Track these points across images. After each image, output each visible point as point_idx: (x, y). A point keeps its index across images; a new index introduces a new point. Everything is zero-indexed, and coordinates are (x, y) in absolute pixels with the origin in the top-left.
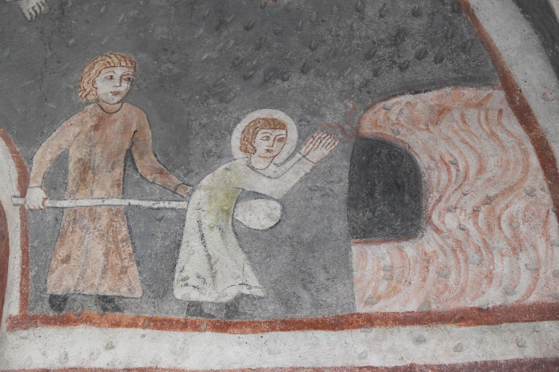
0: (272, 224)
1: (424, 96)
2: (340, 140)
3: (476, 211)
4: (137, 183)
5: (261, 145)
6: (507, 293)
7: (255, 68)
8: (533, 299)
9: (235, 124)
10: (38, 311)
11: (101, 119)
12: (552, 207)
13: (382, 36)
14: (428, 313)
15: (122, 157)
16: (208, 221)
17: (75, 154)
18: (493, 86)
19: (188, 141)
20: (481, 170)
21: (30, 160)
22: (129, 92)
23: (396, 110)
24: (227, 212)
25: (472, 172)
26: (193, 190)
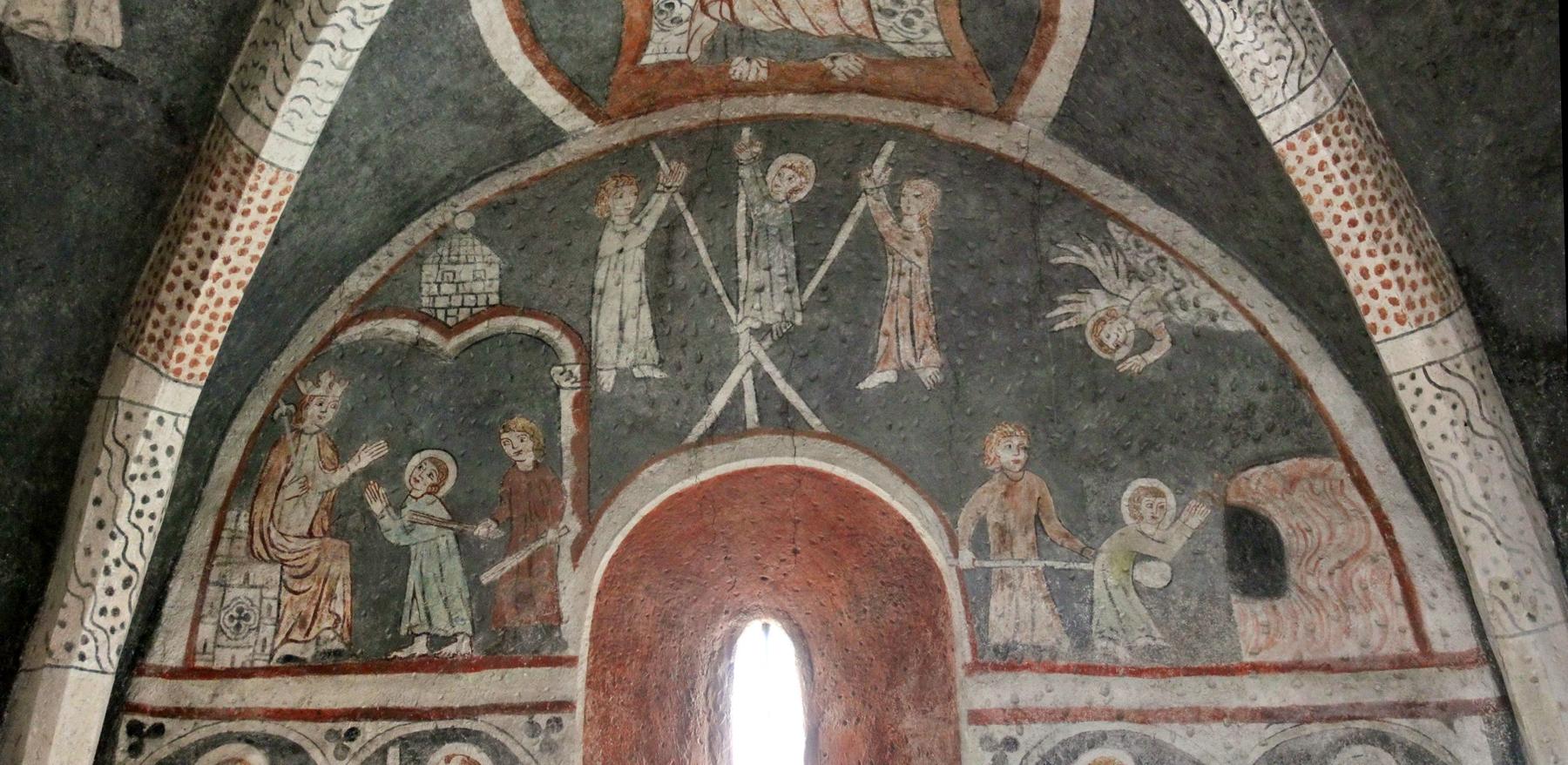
0: (1165, 583)
1: (1275, 465)
2: (1212, 508)
3: (1331, 574)
4: (1048, 546)
5: (1147, 513)
6: (1364, 645)
7: (1131, 439)
8: (1384, 651)
9: (1122, 492)
10: (986, 658)
11: (1009, 487)
12: (1393, 571)
13: (1236, 410)
14: (1301, 662)
15: (1032, 522)
16: (1111, 581)
17: (992, 518)
18: (1334, 458)
19: (1084, 507)
20: (1332, 536)
21: (955, 523)
22: (1027, 461)
23: (1254, 480)
24: (1127, 571)
25: (1324, 539)
26: (1097, 553)
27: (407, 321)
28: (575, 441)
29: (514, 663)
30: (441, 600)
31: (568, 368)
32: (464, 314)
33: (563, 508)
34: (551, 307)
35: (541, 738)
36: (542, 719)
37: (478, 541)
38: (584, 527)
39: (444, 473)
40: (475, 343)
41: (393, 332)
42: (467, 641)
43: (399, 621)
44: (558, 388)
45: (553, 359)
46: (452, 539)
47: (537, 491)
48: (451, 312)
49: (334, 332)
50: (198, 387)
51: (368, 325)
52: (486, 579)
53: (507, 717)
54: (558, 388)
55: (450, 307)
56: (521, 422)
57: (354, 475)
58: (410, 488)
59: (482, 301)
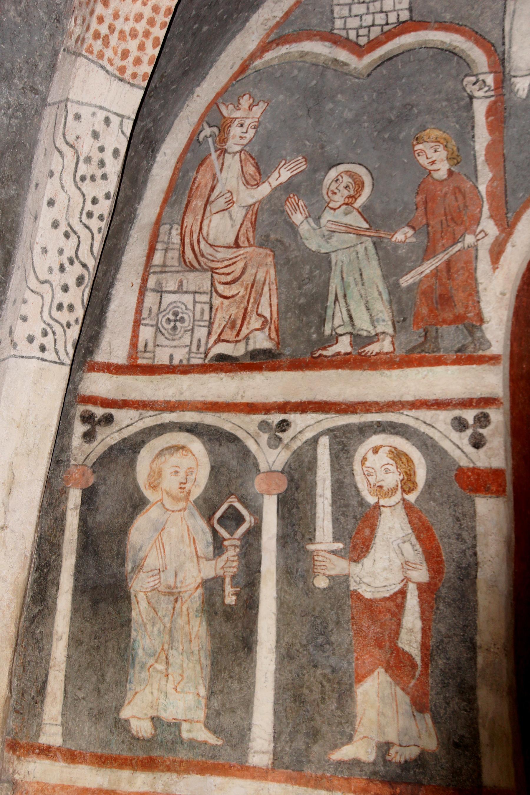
27: (320, 43)
28: (489, 149)
29: (439, 362)
30: (363, 303)
31: (481, 77)
32: (375, 32)
33: (481, 212)
34: (462, 18)
35: (469, 432)
36: (469, 415)
37: (396, 247)
38: (502, 231)
39: (360, 185)
40: (389, 59)
41: (307, 53)
42: (388, 339)
43: (323, 322)
44: (471, 98)
45: (467, 71)
46: (371, 246)
47: (453, 198)
48: (362, 32)
49: (253, 57)
50: (139, 87)
51: (283, 50)
52: (406, 281)
53: (433, 412)
54: (471, 98)
55: (361, 27)
56: (435, 133)
57: (276, 189)
58: (328, 200)
59: (393, 18)
